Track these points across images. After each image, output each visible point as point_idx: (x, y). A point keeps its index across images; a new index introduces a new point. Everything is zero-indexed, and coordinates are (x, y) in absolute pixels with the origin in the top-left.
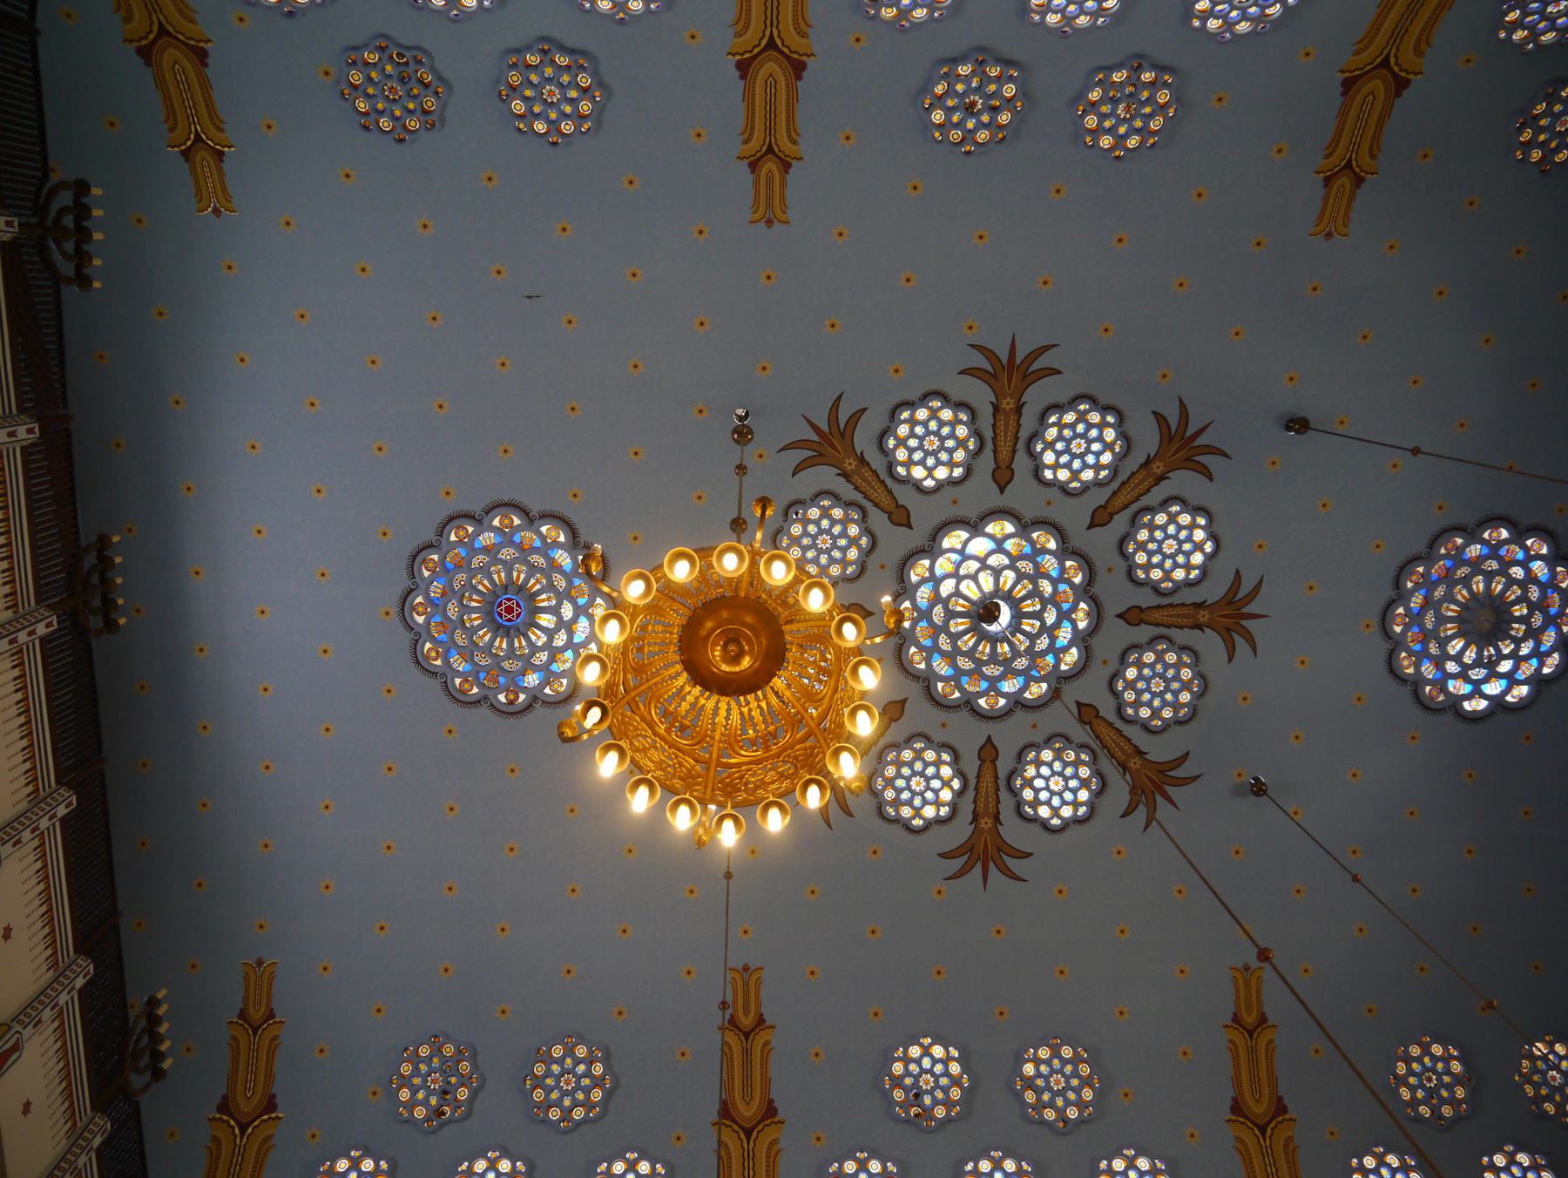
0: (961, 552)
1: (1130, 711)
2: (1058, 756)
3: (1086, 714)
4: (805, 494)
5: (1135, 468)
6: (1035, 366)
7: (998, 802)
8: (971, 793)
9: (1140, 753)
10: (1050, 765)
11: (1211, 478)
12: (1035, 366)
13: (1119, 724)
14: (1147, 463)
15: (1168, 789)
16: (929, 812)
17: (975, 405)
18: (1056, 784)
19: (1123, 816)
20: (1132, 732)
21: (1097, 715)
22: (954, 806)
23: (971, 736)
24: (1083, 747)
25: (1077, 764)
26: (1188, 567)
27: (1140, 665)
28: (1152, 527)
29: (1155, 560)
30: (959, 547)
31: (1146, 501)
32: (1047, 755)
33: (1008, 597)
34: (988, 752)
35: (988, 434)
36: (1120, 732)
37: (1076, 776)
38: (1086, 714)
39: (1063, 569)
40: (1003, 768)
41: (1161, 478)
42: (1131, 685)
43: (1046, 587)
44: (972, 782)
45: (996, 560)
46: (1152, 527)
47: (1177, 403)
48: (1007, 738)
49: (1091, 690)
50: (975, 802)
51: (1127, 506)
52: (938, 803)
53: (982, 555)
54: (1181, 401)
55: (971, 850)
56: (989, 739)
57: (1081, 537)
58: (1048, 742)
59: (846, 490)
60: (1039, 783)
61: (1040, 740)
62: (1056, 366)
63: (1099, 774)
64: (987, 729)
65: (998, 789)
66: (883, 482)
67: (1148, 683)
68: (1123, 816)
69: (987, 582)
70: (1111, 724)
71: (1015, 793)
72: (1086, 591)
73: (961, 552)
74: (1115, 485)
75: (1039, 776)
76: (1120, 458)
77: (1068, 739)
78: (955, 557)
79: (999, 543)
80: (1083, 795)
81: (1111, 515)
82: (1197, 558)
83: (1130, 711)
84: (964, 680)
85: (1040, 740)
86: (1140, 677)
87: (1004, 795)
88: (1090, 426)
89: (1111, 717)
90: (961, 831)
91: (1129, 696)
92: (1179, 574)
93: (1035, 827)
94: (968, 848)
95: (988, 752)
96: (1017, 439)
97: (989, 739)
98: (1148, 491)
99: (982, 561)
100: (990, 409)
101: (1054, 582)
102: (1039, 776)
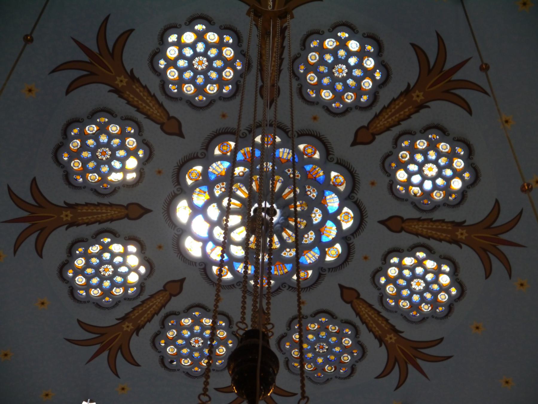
0: (205, 242)
1: (364, 98)
2: (404, 166)
3: (363, 137)
4: (155, 357)
5: (123, 102)
6: (30, 200)
7: (443, 221)
8: (432, 243)
9: (408, 91)
10: (411, 174)
11: (132, 31)
12: (30, 200)
13: (377, 109)
14: (117, 91)
15: (448, 66)
16: (445, 280)
17: (69, 241)
18: (431, 170)
19: (470, 112)
20: (385, 99)
21: (367, 128)
22: (441, 259)
23: (378, 237)
24: (396, 144)
25: (413, 151)
26: (220, 45)
27: (319, 87)
28: (181, 82)
29: (213, 75)
30: (201, 244)
31: (155, 89)
32: (401, 175)
33: (246, 204)
34: (394, 224)
35: (96, 227)
36: (384, 108)
37: (424, 153)
38: (363, 137)
39: (222, 158)
40: (408, 213)
41: (132, 77)
42: (338, 96)
43: (239, 170)
44: (422, 240)
45: (213, 212)
46: (181, 82)
47: (56, 74)
48: (381, 208)
49: (341, 133)
50: (440, 240)
51: (161, 105)
52: (438, 272)
53: (207, 226)
54: (54, 71)
55: (485, 250)
56: (382, 222)
57: (191, 144)
58: (391, 175)
59: (153, 327)
60: (428, 185)
61: (387, 180)
62: (28, 184)
63: (423, 132)
64: (372, 222)
65: (431, 220)
66: (143, 302)
67: (338, 80)
68: (470, 112)
69: (234, 220)
70: (376, 116)
71: (437, 206)
72: (243, 137)
73: (205, 242)
74: (140, 117)
75: (420, 185)
76: (113, 116)
77: (388, 156)
78: (210, 245)
79: (196, 211)
80: (444, 147)
81: (170, 118)
82: (212, 37)
83: (364, 98)
84: (325, 239)
85: (387, 180)
86: (331, 87)
87: (436, 215)
88: (84, 147)
89: (369, 115)
90: (467, 256)
91: (349, 98)
92: (228, 52)
93: (470, 194)
94: (484, 254)
95: (394, 224)
96: (99, 204)
97: (382, 222)
98: (145, 87)
99: (213, 224)
100: (74, 229)
101: (234, 164)
102: (420, 185)
